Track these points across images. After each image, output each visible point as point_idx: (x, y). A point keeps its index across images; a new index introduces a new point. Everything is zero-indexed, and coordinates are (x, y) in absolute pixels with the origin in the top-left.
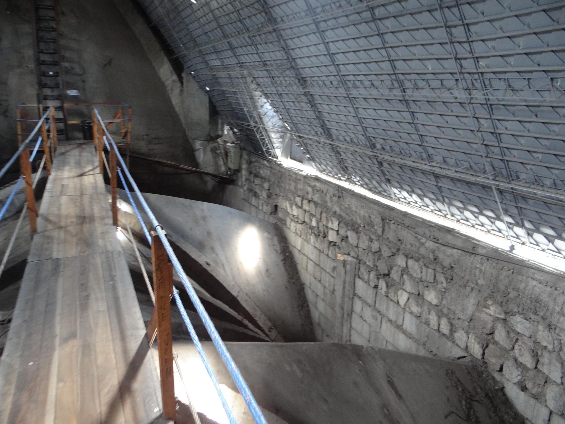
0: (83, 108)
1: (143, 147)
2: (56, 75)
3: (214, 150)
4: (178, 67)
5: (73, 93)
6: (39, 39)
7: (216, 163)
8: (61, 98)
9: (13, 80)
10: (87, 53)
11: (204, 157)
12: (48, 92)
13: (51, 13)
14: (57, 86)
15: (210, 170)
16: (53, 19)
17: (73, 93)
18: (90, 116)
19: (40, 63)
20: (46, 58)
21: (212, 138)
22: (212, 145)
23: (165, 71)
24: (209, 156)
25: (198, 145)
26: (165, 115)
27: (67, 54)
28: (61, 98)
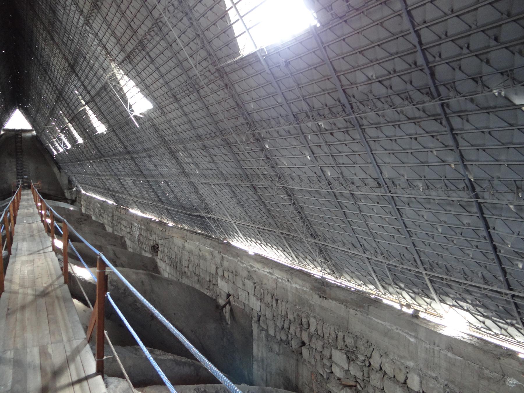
0: (29, 181)
1: (47, 191)
2: (22, 172)
3: (70, 192)
4: (59, 169)
5: (26, 177)
6: (17, 163)
7: (72, 197)
8: (23, 178)
9: (9, 175)
10: (30, 166)
11: (67, 195)
12: (19, 177)
13: (20, 156)
14: (22, 175)
15: (69, 198)
16: (22, 158)
17: (26, 177)
18: (30, 183)
19: (17, 169)
20: (19, 168)
21: (70, 189)
22: (70, 191)
23: (55, 170)
24: (69, 194)
25: (65, 191)
26: (54, 181)
27: (24, 166)
28: (23, 178)
